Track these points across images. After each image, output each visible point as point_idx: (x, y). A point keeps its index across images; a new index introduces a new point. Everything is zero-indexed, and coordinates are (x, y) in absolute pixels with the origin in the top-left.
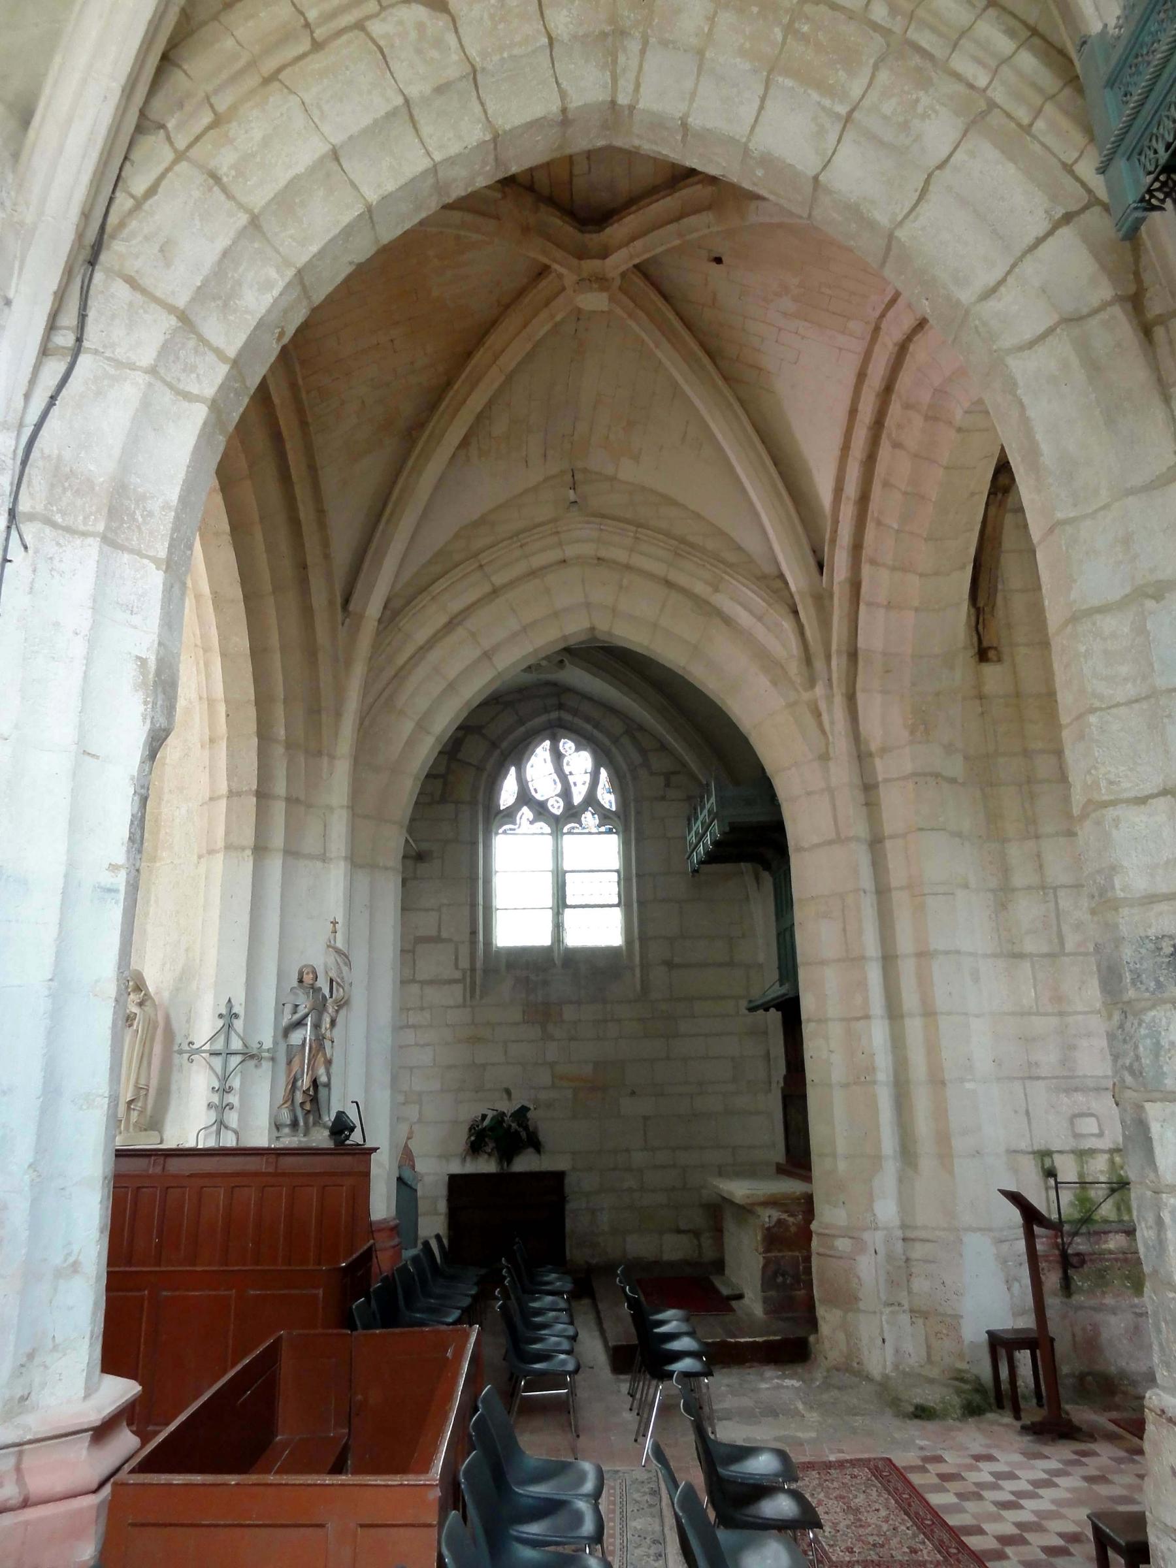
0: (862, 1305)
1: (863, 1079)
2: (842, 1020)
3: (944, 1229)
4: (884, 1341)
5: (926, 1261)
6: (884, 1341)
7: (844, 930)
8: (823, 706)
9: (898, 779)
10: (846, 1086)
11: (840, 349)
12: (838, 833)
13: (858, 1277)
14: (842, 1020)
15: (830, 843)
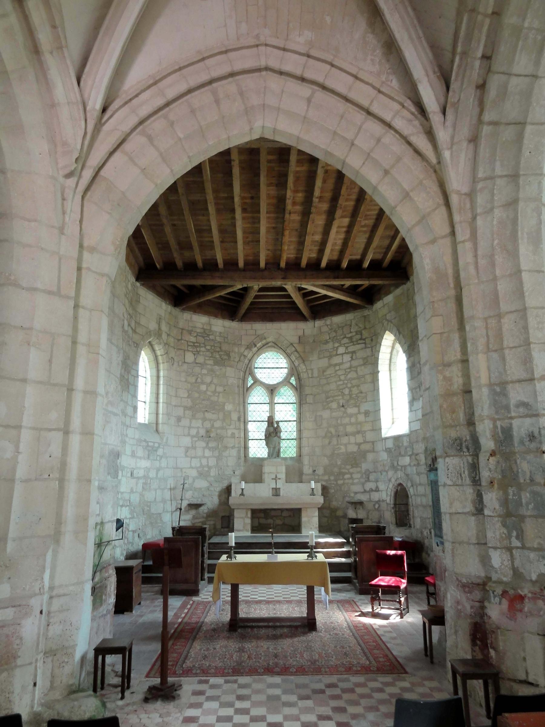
0: (19, 662)
1: (47, 476)
2: (34, 428)
3: (74, 585)
4: (35, 684)
5: (61, 611)
6: (35, 684)
7: (50, 361)
8: (69, 194)
9: (96, 272)
10: (27, 481)
11: (225, 26)
12: (59, 288)
13: (21, 639)
14: (34, 428)
15: (50, 293)
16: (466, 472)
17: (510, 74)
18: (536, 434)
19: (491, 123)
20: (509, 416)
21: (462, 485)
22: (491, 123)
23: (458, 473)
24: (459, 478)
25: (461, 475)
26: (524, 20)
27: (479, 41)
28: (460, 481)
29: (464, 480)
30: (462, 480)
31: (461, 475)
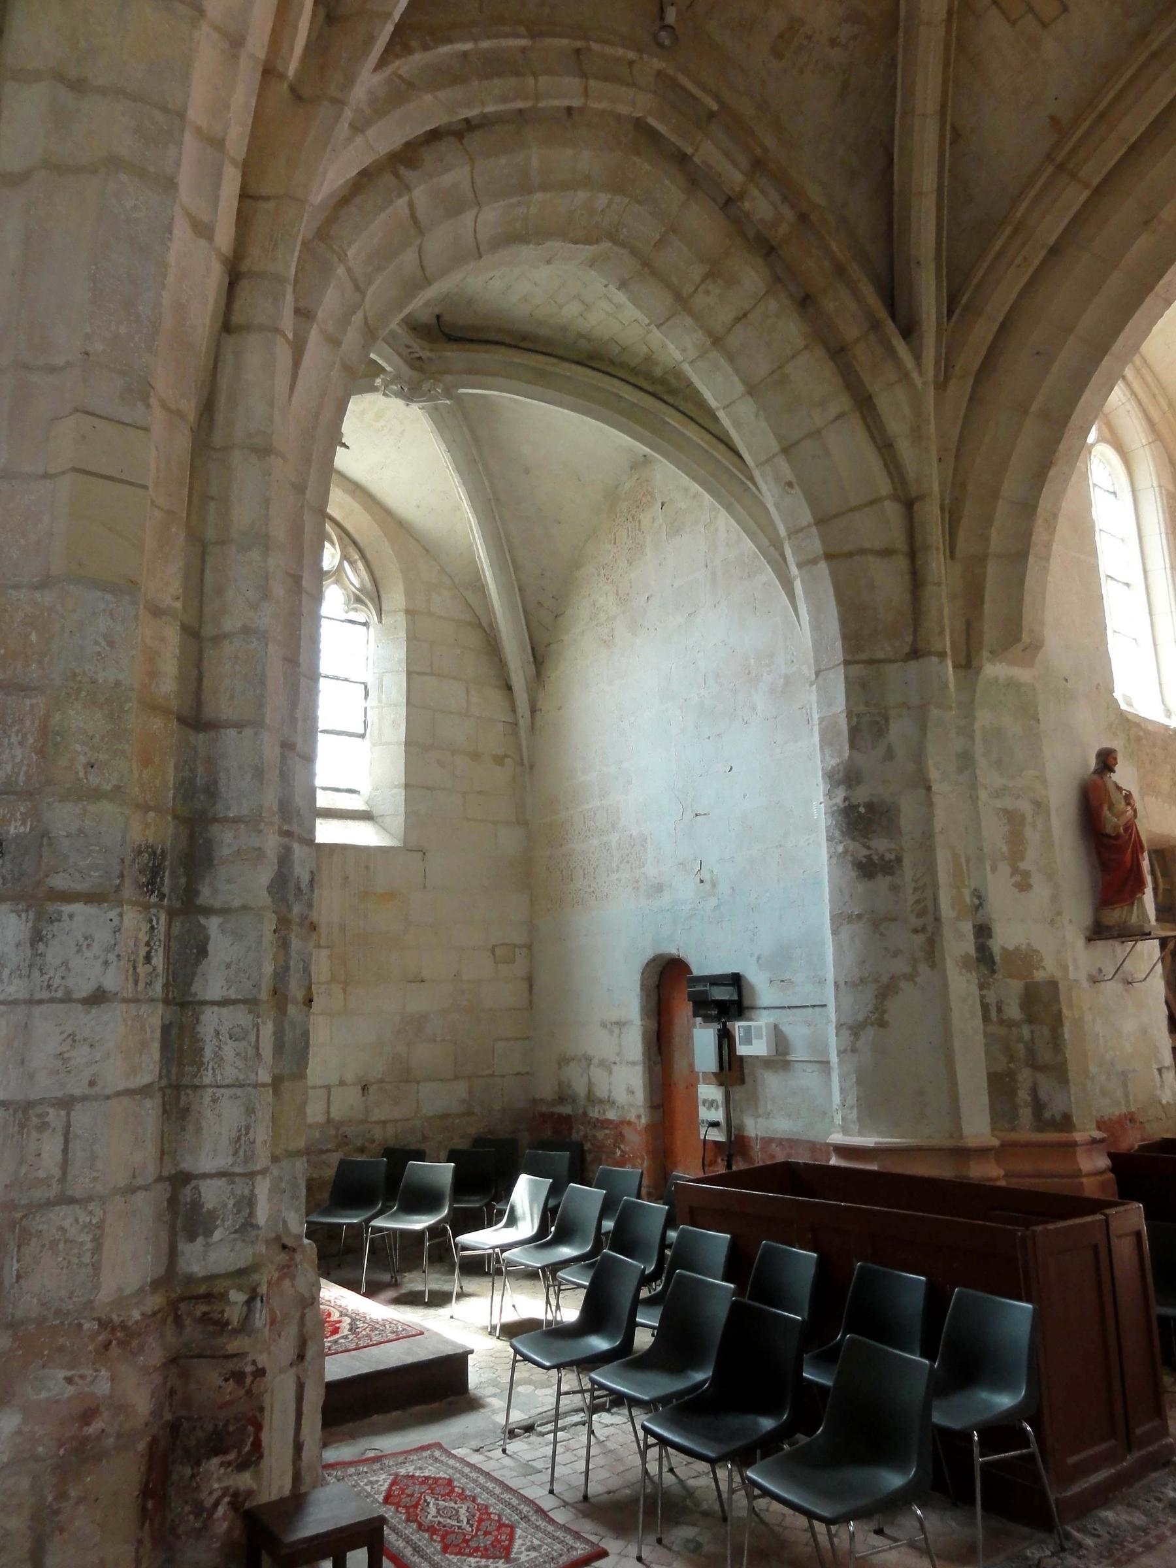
16: (158, 960)
17: (479, 204)
18: (303, 886)
19: (411, 206)
20: (285, 828)
21: (136, 1001)
22: (411, 206)
23: (129, 960)
24: (130, 978)
25: (135, 968)
26: (545, 187)
27: (504, 99)
28: (130, 985)
29: (141, 985)
30: (136, 983)
31: (135, 968)
